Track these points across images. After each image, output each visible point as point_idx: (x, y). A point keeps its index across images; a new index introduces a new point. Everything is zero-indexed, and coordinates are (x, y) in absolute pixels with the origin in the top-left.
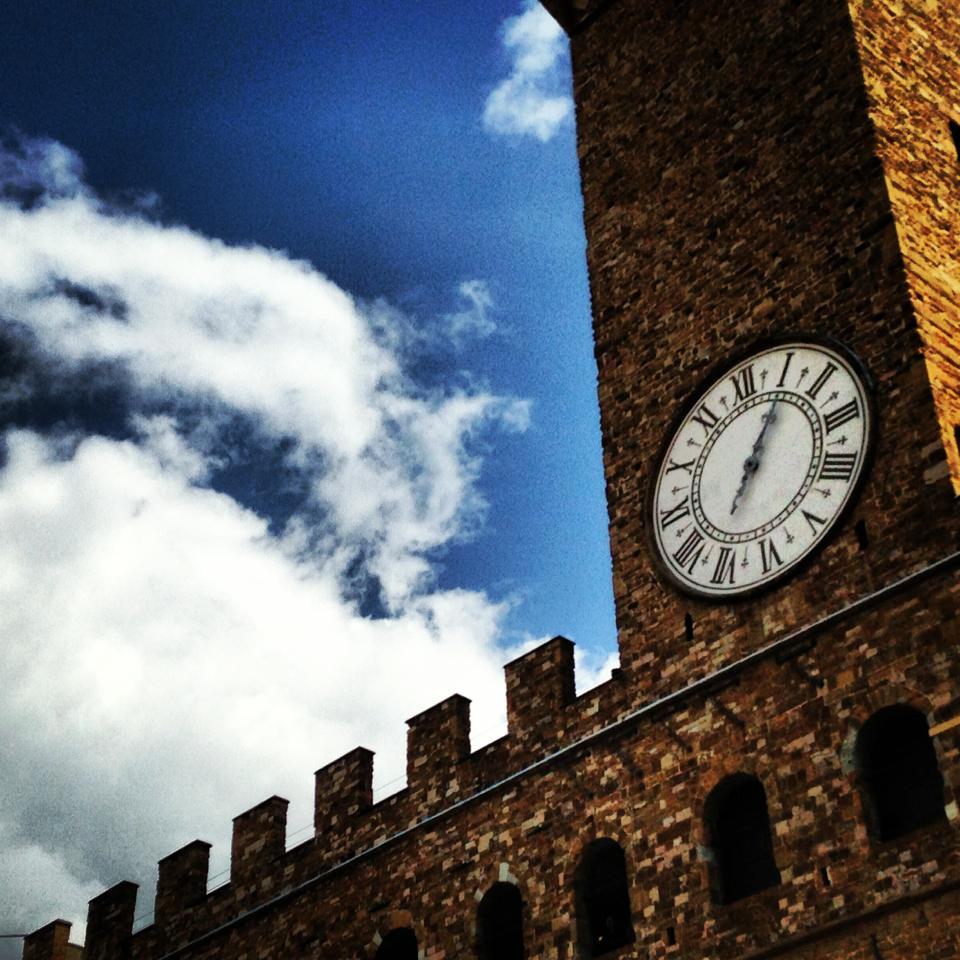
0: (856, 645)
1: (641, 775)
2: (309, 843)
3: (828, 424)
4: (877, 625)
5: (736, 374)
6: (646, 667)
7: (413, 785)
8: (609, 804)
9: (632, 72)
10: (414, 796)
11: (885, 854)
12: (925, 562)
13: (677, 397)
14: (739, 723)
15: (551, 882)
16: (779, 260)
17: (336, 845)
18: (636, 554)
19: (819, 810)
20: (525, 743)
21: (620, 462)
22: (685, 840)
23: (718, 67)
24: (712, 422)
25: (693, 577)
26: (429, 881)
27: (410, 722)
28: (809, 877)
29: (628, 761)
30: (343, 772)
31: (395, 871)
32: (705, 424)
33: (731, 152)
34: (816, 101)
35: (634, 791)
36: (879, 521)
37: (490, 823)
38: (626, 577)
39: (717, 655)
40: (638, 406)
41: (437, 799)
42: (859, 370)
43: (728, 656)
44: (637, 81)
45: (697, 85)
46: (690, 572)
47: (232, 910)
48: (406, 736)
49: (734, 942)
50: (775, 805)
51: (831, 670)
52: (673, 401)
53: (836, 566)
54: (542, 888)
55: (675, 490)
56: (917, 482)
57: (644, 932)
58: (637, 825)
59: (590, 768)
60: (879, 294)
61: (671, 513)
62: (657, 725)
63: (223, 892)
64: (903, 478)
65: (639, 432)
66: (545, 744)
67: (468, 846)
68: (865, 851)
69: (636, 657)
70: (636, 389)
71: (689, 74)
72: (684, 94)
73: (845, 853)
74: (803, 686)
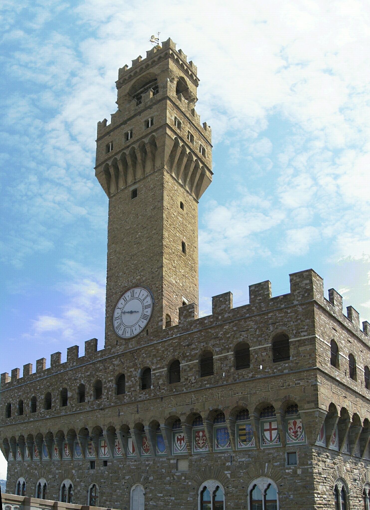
0: (142, 354)
14: (123, 363)
19: (133, 382)
36: (151, 330)
39: (120, 349)
42: (152, 298)
50: (126, 380)
56: (157, 324)
68: (138, 391)
73: (135, 390)
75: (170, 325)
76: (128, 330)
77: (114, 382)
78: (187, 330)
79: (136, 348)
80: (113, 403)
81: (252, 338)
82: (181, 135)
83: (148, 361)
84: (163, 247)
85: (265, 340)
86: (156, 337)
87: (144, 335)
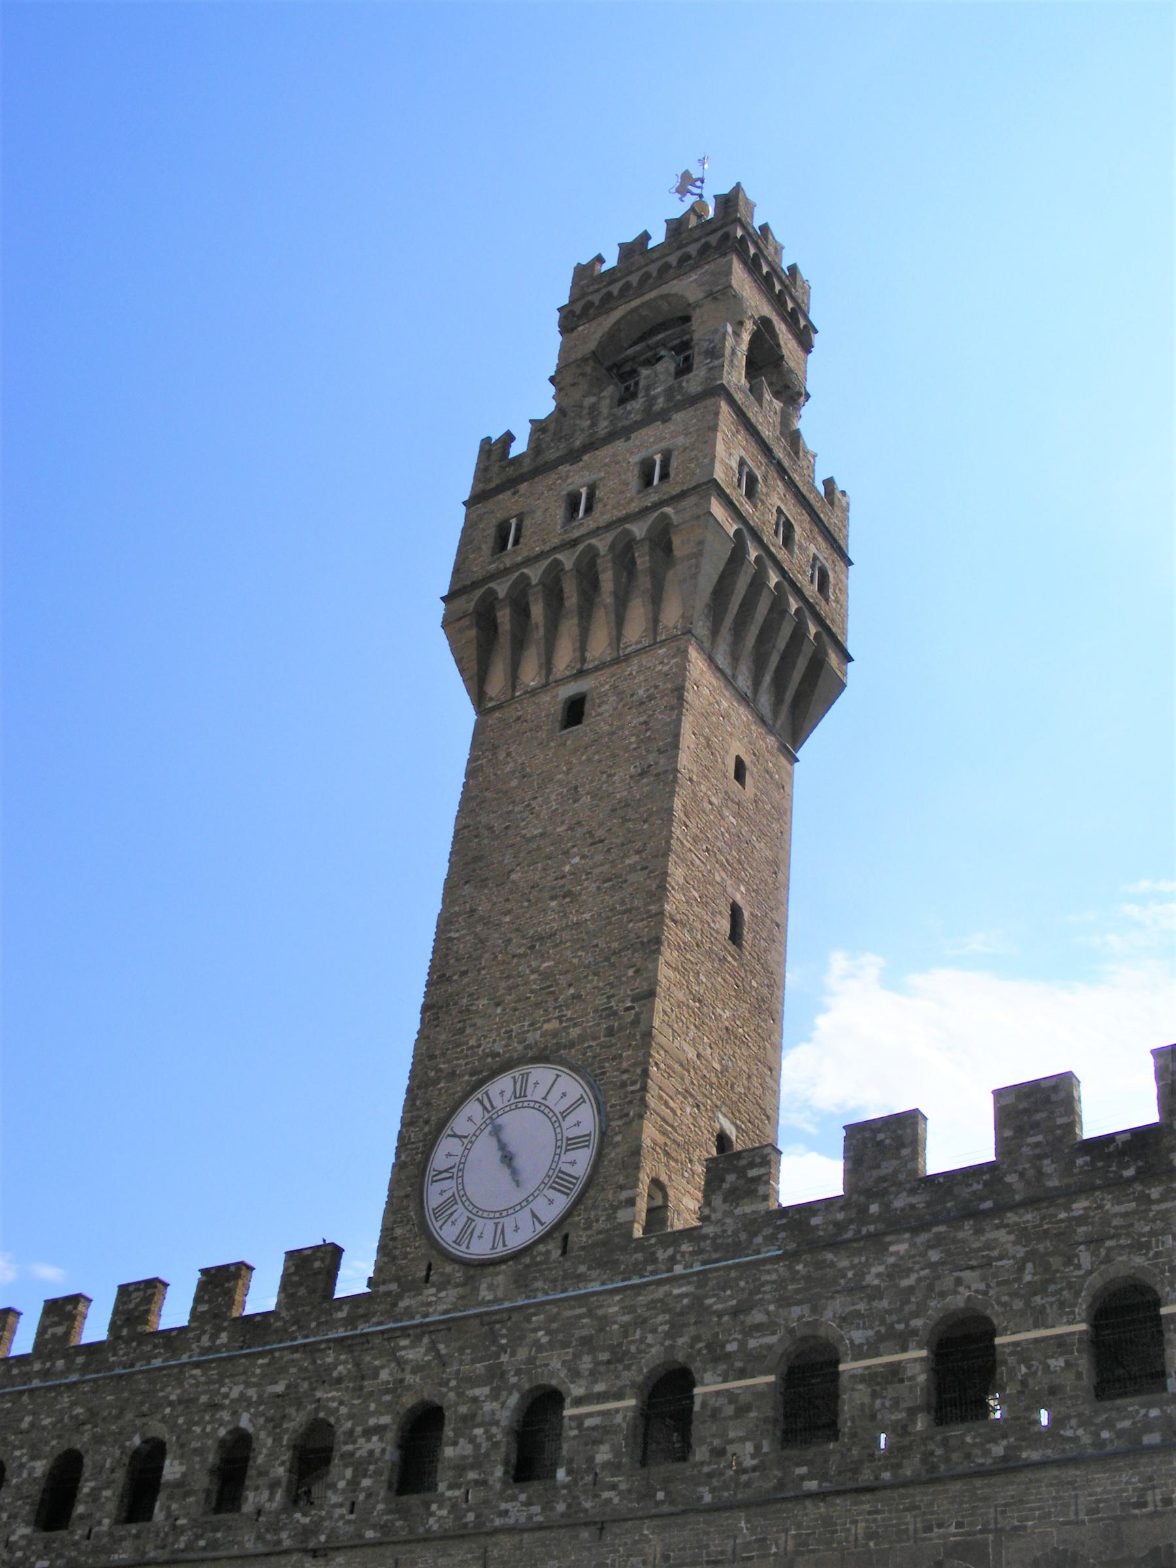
1: (363, 1378)
2: (101, 1343)
3: (568, 1145)
4: (554, 1318)
5: (517, 1075)
6: (388, 1294)
7: (193, 1325)
8: (334, 1393)
9: (513, 772)
10: (191, 1335)
11: (510, 1492)
12: (598, 1283)
13: (471, 1075)
15: (277, 1440)
16: (572, 991)
17: (121, 1353)
18: (407, 1196)
19: (477, 1446)
20: (286, 1322)
21: (415, 1113)
22: (381, 1439)
23: (574, 802)
24: (490, 1108)
25: (441, 1233)
26: (187, 1407)
27: (204, 1272)
28: (457, 1493)
29: (357, 1364)
30: (141, 1293)
31: (162, 1390)
32: (485, 1108)
33: (564, 880)
34: (632, 868)
35: (354, 1389)
36: (579, 1238)
37: (243, 1378)
38: (394, 1213)
39: (439, 1303)
40: (441, 1070)
41: (208, 1344)
43: (450, 1307)
44: (514, 783)
45: (556, 809)
46: (441, 1228)
47: (27, 1377)
48: (196, 1283)
49: (393, 1525)
50: (448, 1432)
51: (516, 1341)
52: (466, 1078)
53: (541, 1263)
54: (270, 1441)
55: (449, 1155)
56: (610, 1218)
57: (334, 1499)
58: (350, 1416)
59: (329, 1360)
60: (630, 1052)
61: (441, 1172)
62: (386, 1343)
63: (22, 1359)
64: (605, 1210)
65: (436, 1093)
66: (300, 1328)
67: (224, 1390)
68: (498, 1486)
69: (384, 1283)
70: (443, 1055)
71: (553, 797)
72: (544, 814)
73: (484, 1483)
74: (494, 1349)
75: (663, 1222)
76: (486, 1227)
77: (390, 1435)
78: (736, 1248)
79: (507, 1305)
80: (373, 1527)
81: (1005, 1298)
82: (755, 520)
83: (556, 1364)
84: (662, 923)
85: (1062, 1304)
86: (600, 1264)
87: (548, 1252)
